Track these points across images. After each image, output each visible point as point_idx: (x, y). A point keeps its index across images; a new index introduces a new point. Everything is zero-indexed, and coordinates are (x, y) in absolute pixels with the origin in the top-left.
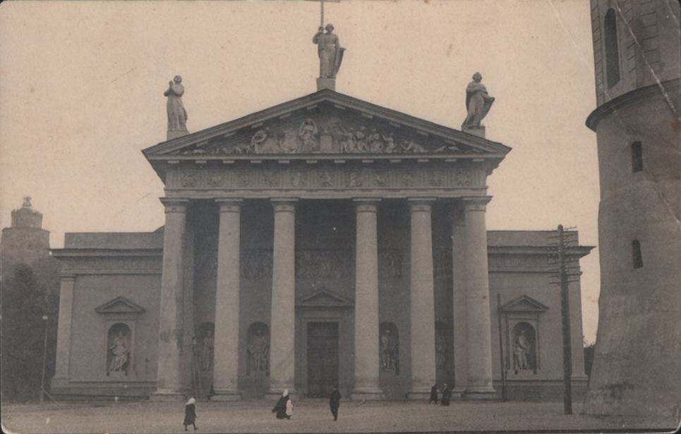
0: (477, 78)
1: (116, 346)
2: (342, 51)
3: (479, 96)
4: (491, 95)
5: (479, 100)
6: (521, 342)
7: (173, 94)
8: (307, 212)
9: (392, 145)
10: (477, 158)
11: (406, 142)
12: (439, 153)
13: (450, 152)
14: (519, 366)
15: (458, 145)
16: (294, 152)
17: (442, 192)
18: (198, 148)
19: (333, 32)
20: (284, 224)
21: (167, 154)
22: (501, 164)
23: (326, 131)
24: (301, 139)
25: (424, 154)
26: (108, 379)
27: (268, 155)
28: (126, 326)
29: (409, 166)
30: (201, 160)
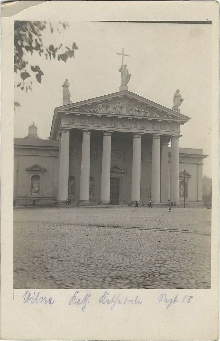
0: (178, 91)
2: (130, 75)
3: (178, 98)
4: (182, 98)
5: (178, 99)
7: (65, 86)
8: (116, 136)
9: (148, 114)
10: (179, 121)
11: (153, 113)
13: (169, 118)
15: (172, 115)
17: (165, 132)
18: (76, 109)
19: (127, 68)
20: (107, 140)
21: (64, 110)
24: (115, 108)
25: (160, 118)
26: (31, 196)
27: (103, 113)
28: (39, 176)
29: (155, 122)
30: (78, 113)
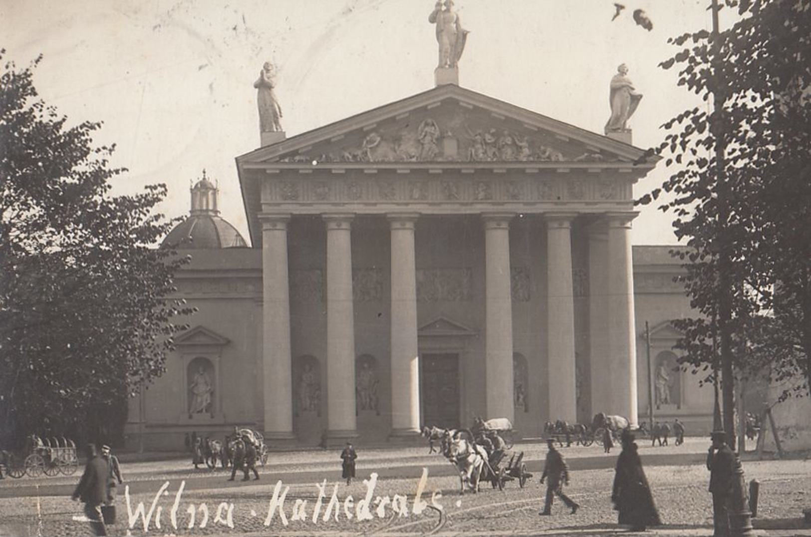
0: (622, 71)
1: (196, 385)
2: (464, 35)
6: (663, 372)
9: (526, 151)
11: (542, 148)
12: (580, 161)
13: (593, 161)
14: (660, 400)
15: (602, 152)
16: (414, 160)
18: (300, 154)
21: (265, 162)
22: (648, 174)
23: (450, 134)
24: (419, 143)
27: (383, 162)
